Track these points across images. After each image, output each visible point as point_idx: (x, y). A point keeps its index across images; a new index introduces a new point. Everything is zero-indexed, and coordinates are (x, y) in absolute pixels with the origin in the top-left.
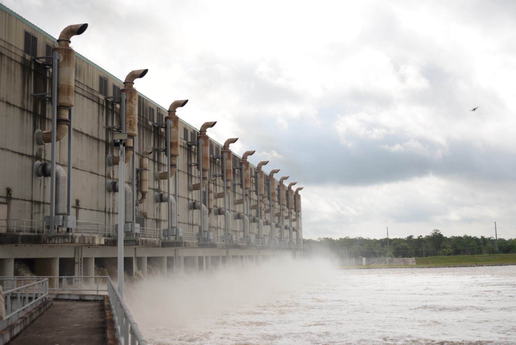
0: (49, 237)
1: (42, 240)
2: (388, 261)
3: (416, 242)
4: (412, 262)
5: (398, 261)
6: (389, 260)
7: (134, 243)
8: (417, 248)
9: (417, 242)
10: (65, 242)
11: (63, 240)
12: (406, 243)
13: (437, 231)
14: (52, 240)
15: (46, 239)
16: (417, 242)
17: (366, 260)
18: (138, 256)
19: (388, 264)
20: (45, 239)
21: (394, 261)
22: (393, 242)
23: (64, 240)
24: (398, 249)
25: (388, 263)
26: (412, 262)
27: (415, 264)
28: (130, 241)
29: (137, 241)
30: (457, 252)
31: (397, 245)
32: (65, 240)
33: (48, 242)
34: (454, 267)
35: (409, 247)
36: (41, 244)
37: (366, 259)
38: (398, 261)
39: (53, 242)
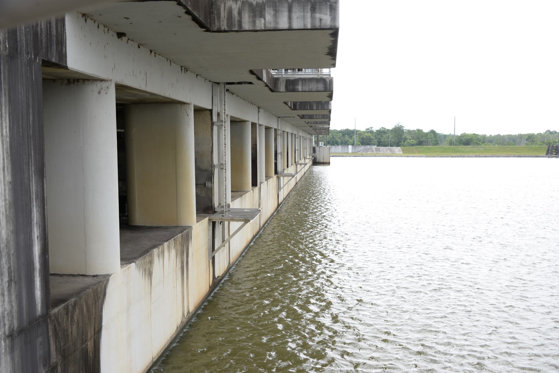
0: (251, 5)
1: (223, 14)
2: (374, 150)
3: (378, 133)
4: (398, 151)
5: (385, 150)
6: (375, 148)
7: (321, 86)
8: (379, 139)
9: (379, 133)
10: (317, 24)
11: (309, 15)
12: (369, 133)
13: (400, 123)
14: (262, 16)
15: (240, 13)
16: (379, 133)
17: (352, 148)
18: (260, 123)
19: (375, 152)
20: (235, 13)
21: (381, 150)
22: (358, 132)
23: (313, 18)
24: (363, 139)
25: (375, 151)
26: (398, 151)
27: (401, 153)
28: (311, 80)
29: (328, 80)
30: (420, 143)
31: (362, 135)
32: (318, 15)
33: (246, 26)
34: (452, 157)
35: (372, 137)
36: (219, 31)
37: (352, 147)
38: (385, 150)
39: (271, 26)
